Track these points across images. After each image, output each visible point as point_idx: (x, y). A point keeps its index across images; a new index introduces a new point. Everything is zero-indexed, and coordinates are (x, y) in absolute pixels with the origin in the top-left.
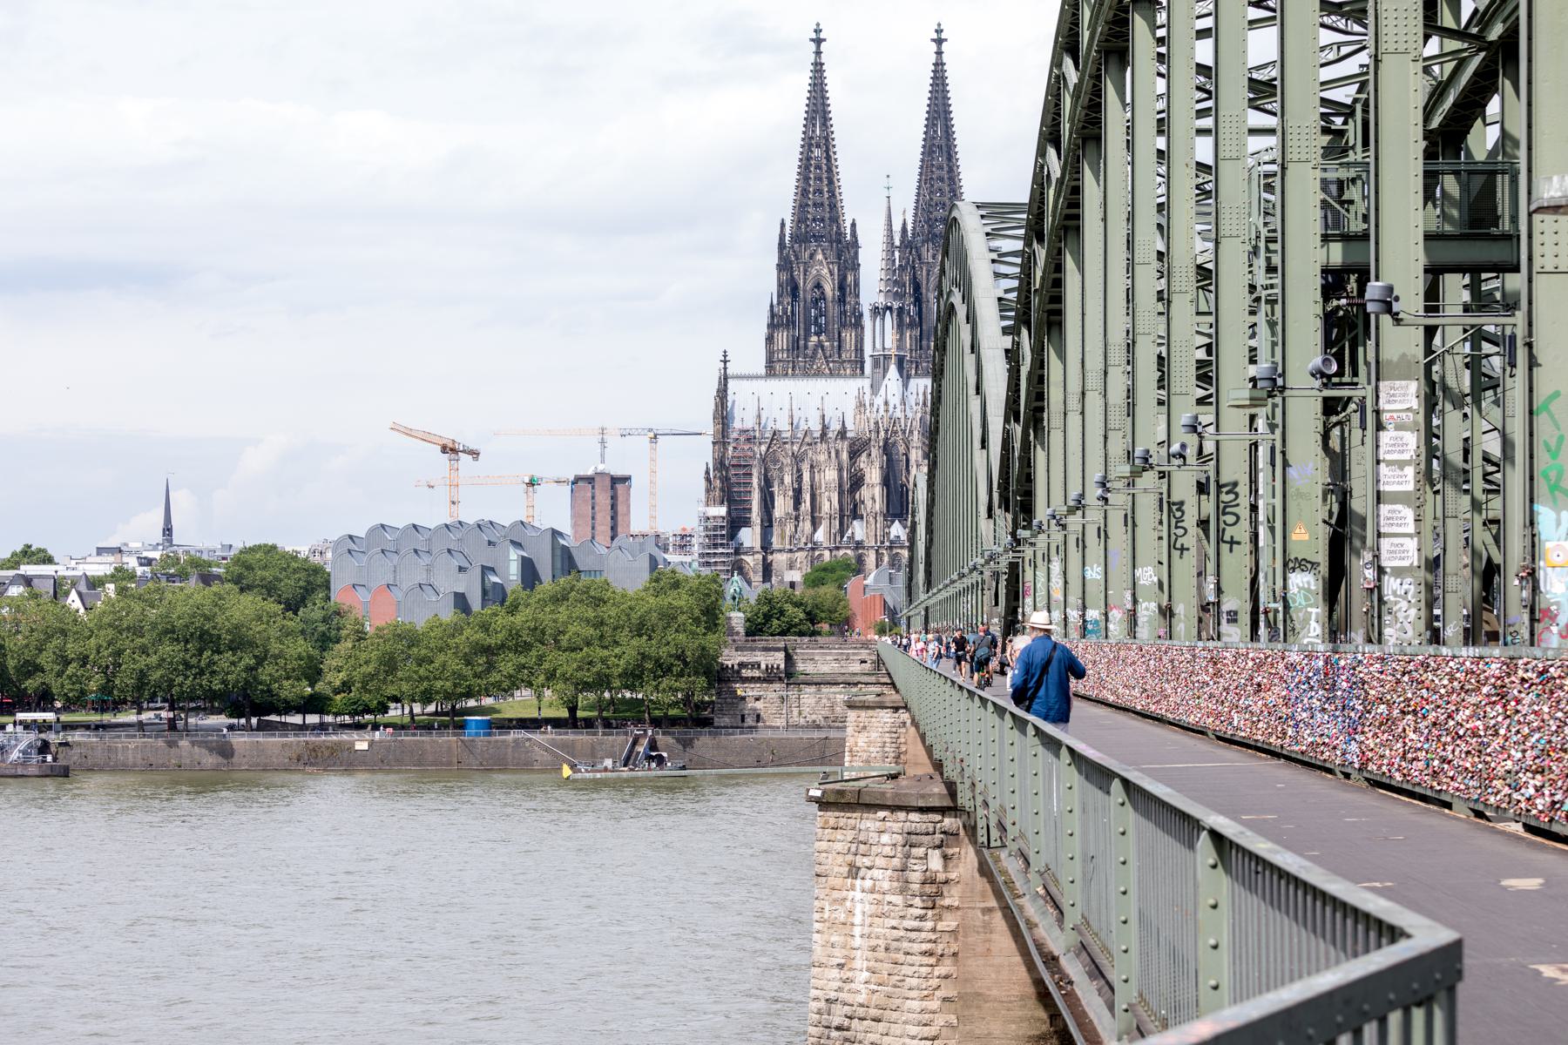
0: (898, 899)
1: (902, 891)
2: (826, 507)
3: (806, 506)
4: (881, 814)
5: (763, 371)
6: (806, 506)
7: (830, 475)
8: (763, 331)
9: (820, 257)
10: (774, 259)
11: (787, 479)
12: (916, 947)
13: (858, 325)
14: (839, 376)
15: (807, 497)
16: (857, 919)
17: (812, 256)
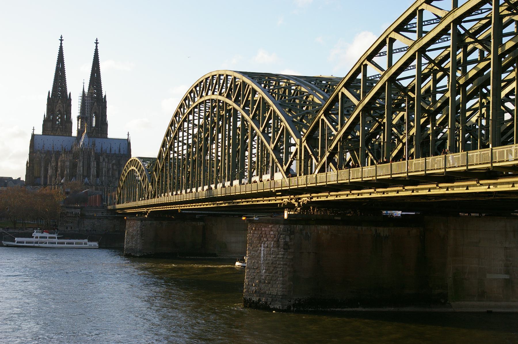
0: (276, 249)
1: (278, 247)
2: (66, 172)
3: (59, 172)
4: (270, 226)
5: (41, 134)
6: (59, 172)
7: (68, 164)
8: (42, 123)
9: (60, 102)
10: (46, 102)
11: (53, 164)
12: (282, 263)
13: (71, 123)
14: (64, 136)
15: (59, 170)
16: (262, 255)
17: (58, 102)
